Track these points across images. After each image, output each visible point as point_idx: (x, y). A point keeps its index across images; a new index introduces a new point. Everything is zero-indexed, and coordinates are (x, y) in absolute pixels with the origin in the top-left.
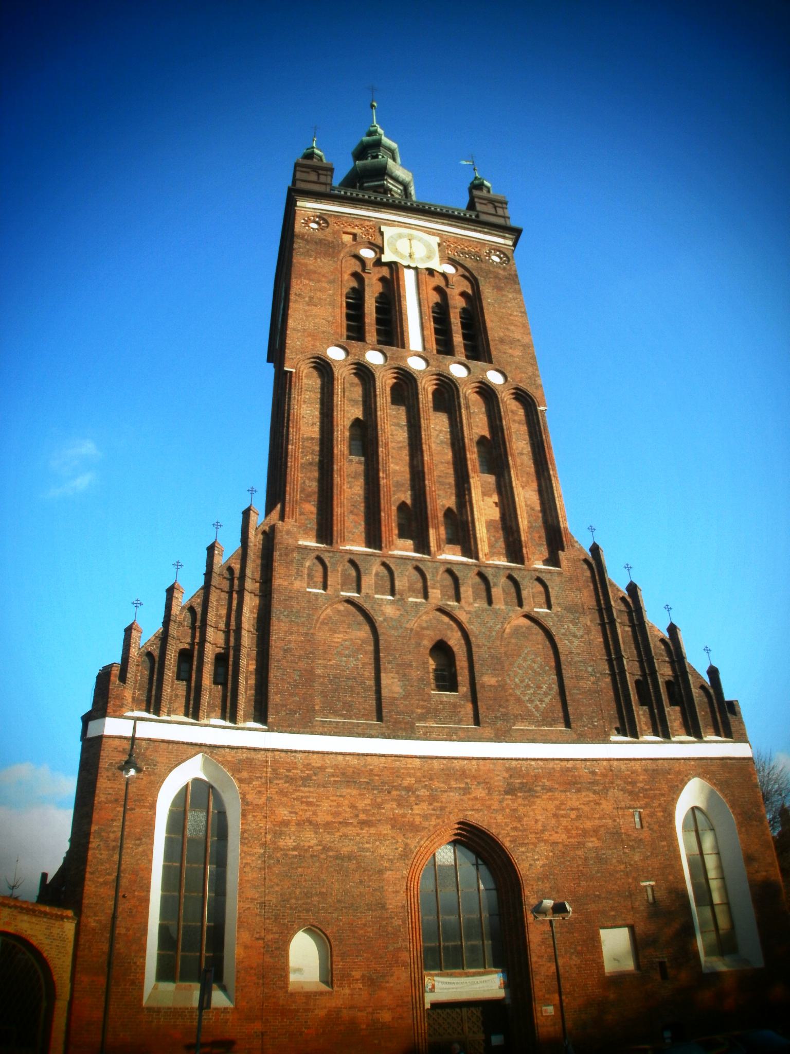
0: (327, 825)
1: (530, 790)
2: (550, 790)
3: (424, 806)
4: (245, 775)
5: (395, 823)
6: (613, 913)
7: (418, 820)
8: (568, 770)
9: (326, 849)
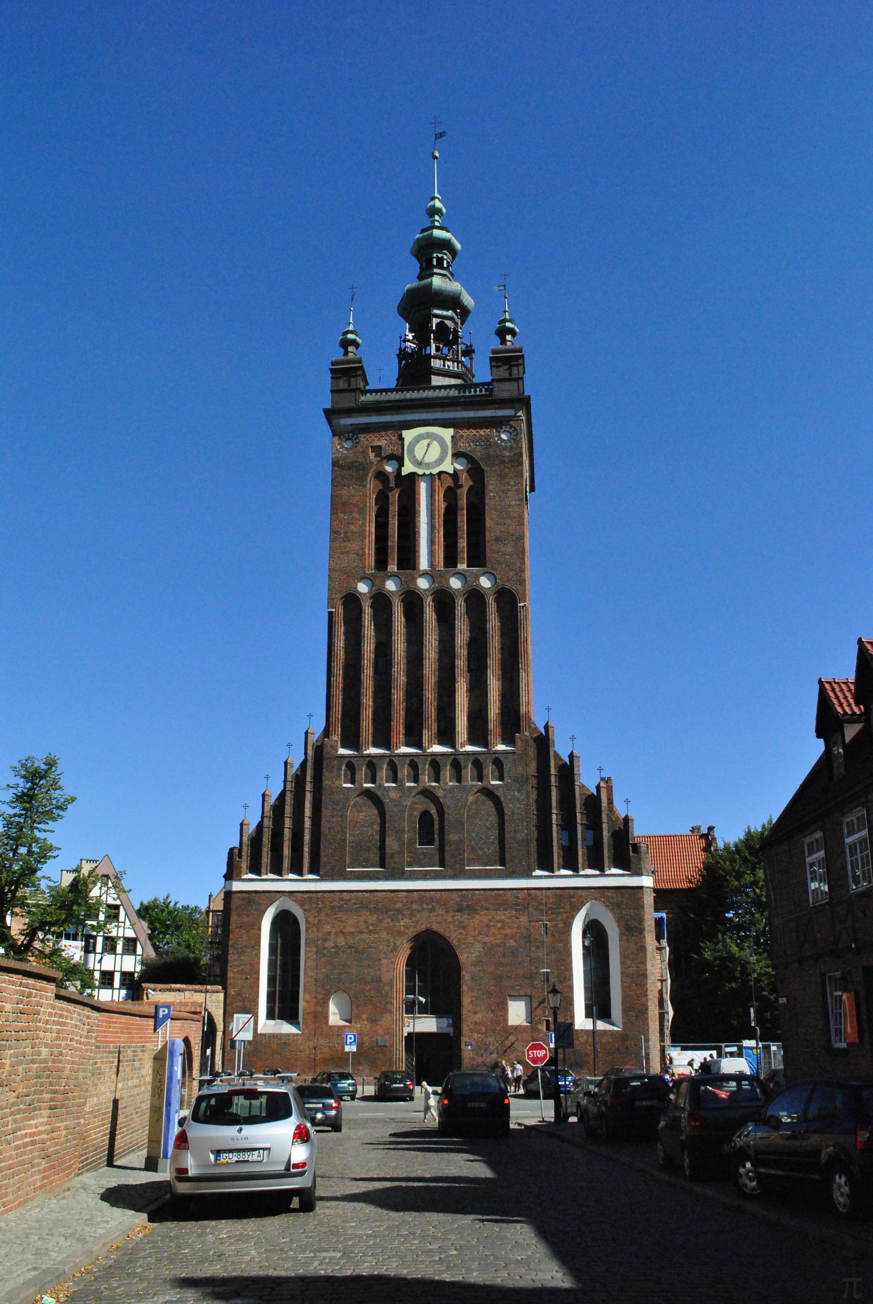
0: (351, 933)
2: (487, 909)
4: (307, 907)
5: (388, 930)
7: (402, 929)
8: (499, 895)
9: (350, 947)
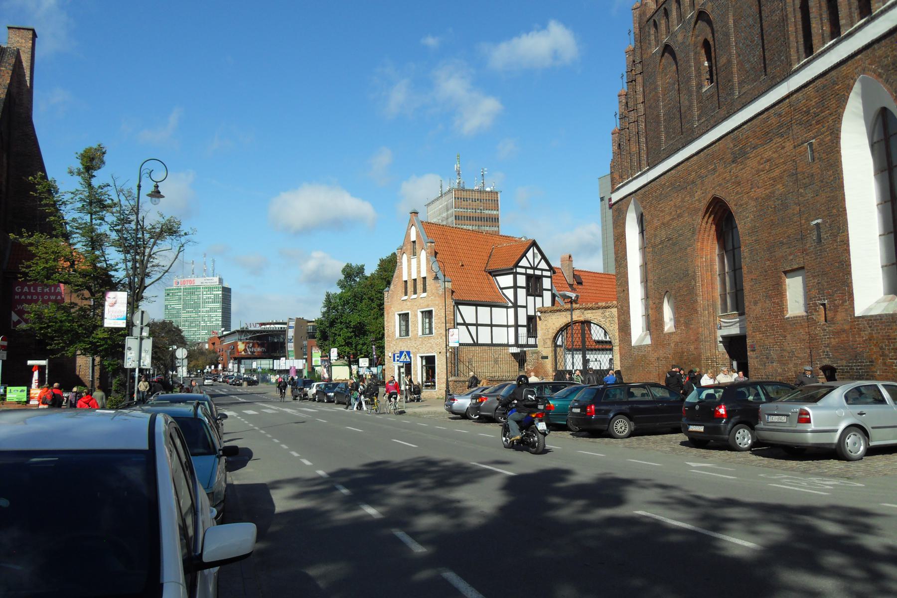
0: (668, 222)
4: (644, 203)
6: (791, 257)
8: (765, 121)
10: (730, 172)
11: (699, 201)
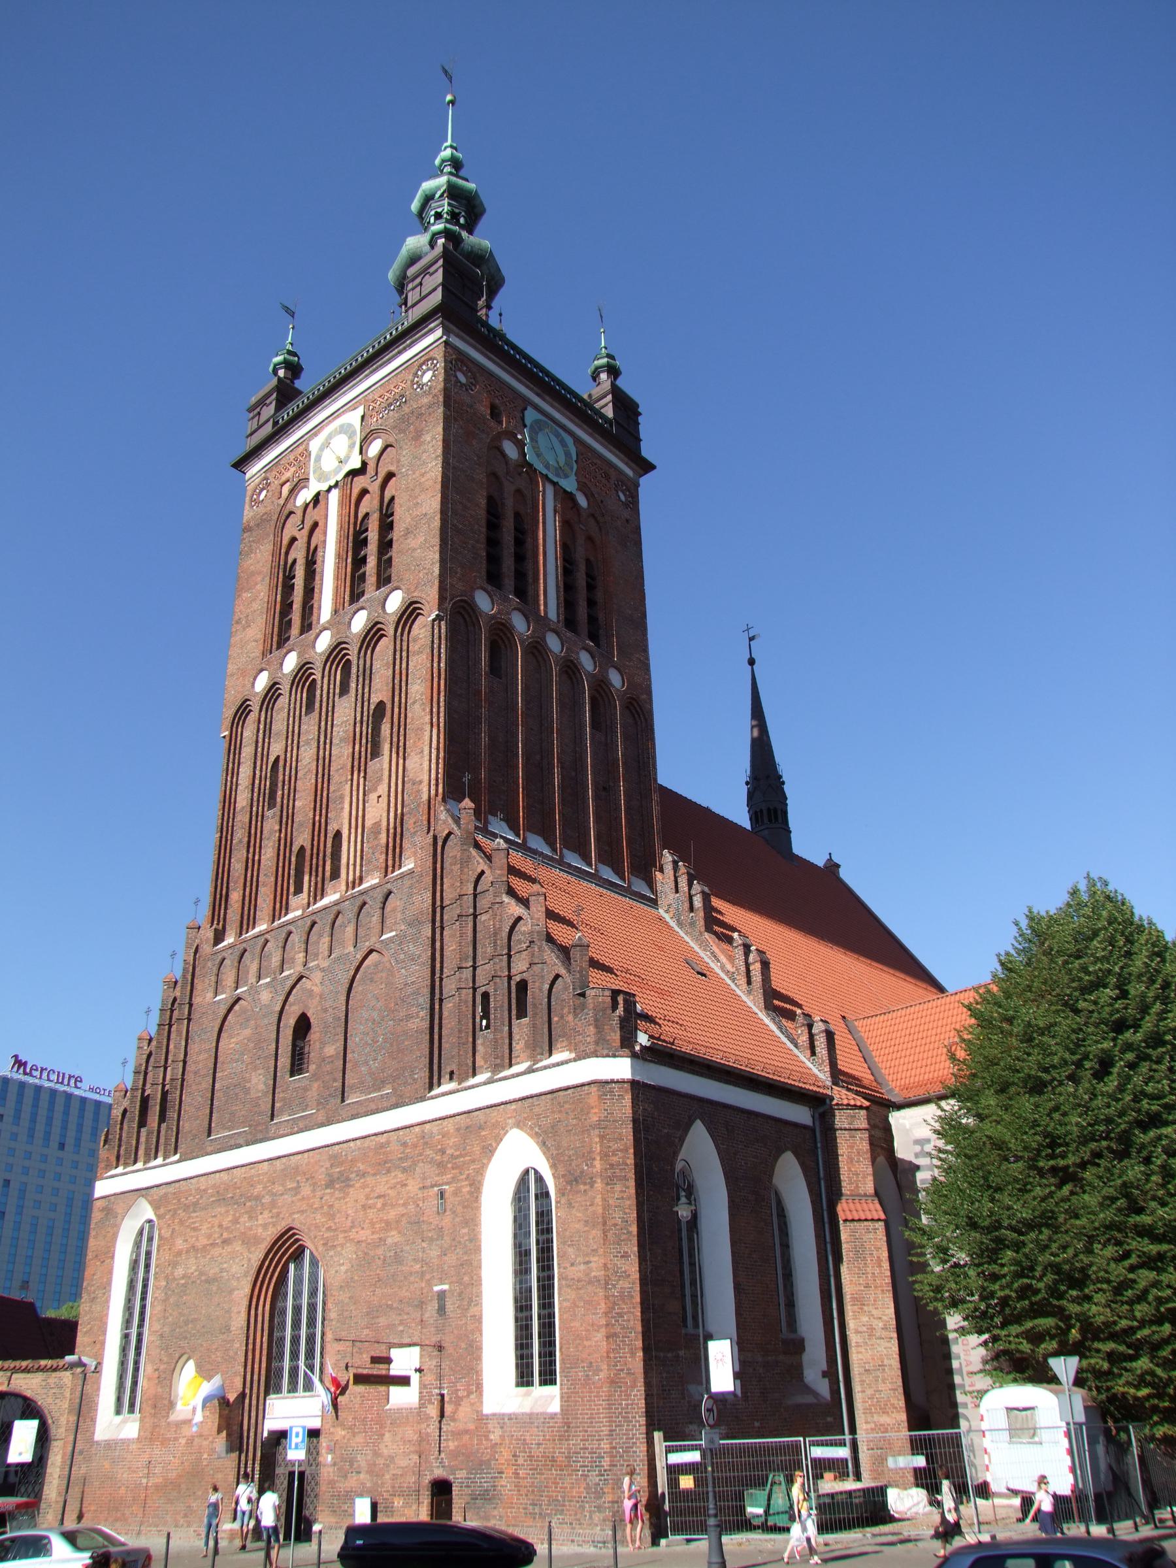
0: (205, 1247)
1: (348, 1179)
3: (266, 1214)
4: (162, 1211)
6: (401, 1328)
8: (382, 1146)
10: (321, 1198)
11: (265, 1226)
